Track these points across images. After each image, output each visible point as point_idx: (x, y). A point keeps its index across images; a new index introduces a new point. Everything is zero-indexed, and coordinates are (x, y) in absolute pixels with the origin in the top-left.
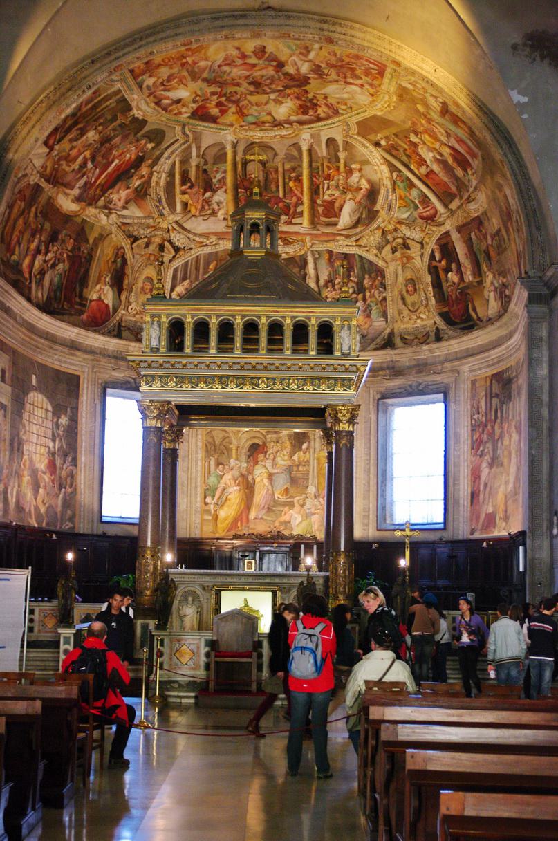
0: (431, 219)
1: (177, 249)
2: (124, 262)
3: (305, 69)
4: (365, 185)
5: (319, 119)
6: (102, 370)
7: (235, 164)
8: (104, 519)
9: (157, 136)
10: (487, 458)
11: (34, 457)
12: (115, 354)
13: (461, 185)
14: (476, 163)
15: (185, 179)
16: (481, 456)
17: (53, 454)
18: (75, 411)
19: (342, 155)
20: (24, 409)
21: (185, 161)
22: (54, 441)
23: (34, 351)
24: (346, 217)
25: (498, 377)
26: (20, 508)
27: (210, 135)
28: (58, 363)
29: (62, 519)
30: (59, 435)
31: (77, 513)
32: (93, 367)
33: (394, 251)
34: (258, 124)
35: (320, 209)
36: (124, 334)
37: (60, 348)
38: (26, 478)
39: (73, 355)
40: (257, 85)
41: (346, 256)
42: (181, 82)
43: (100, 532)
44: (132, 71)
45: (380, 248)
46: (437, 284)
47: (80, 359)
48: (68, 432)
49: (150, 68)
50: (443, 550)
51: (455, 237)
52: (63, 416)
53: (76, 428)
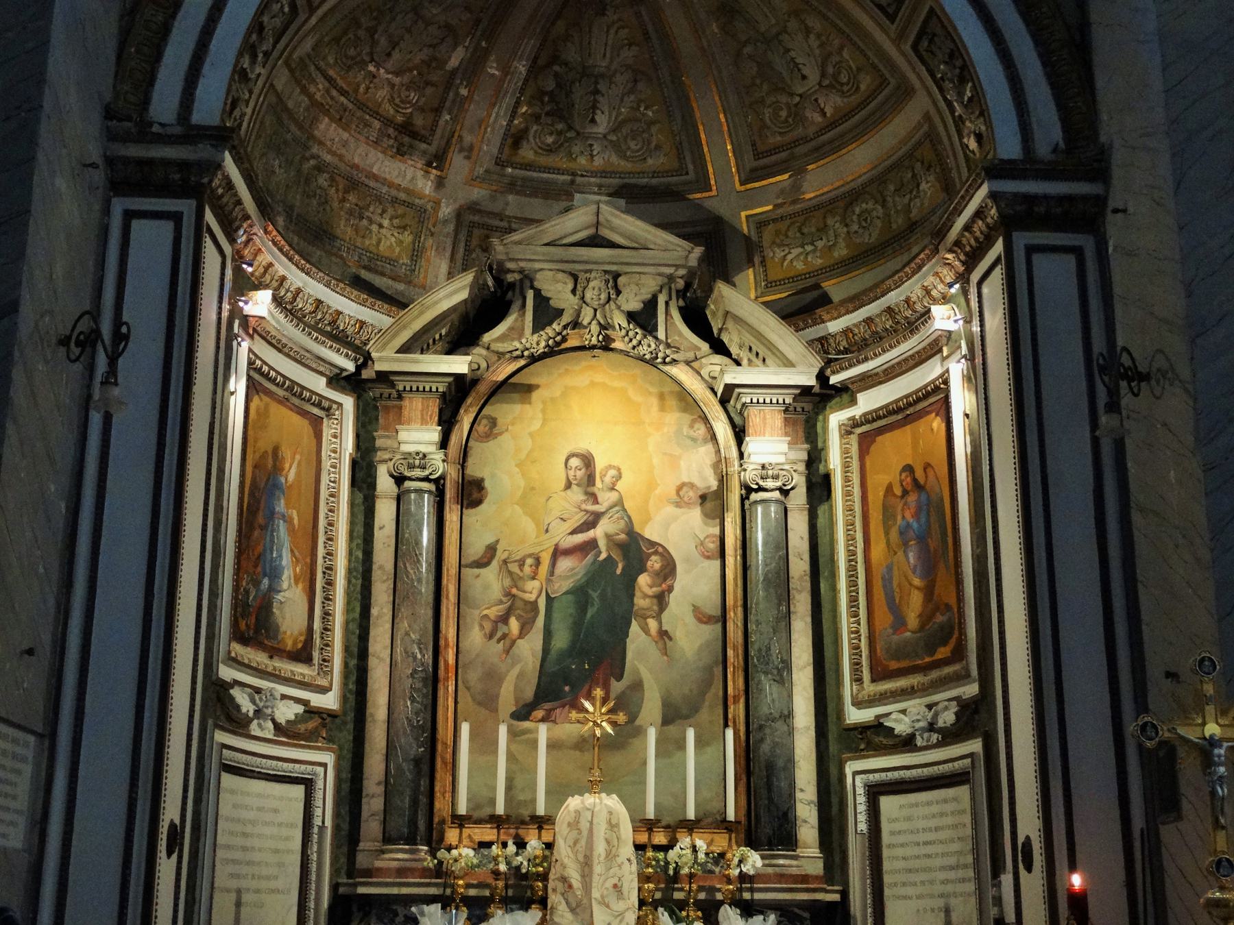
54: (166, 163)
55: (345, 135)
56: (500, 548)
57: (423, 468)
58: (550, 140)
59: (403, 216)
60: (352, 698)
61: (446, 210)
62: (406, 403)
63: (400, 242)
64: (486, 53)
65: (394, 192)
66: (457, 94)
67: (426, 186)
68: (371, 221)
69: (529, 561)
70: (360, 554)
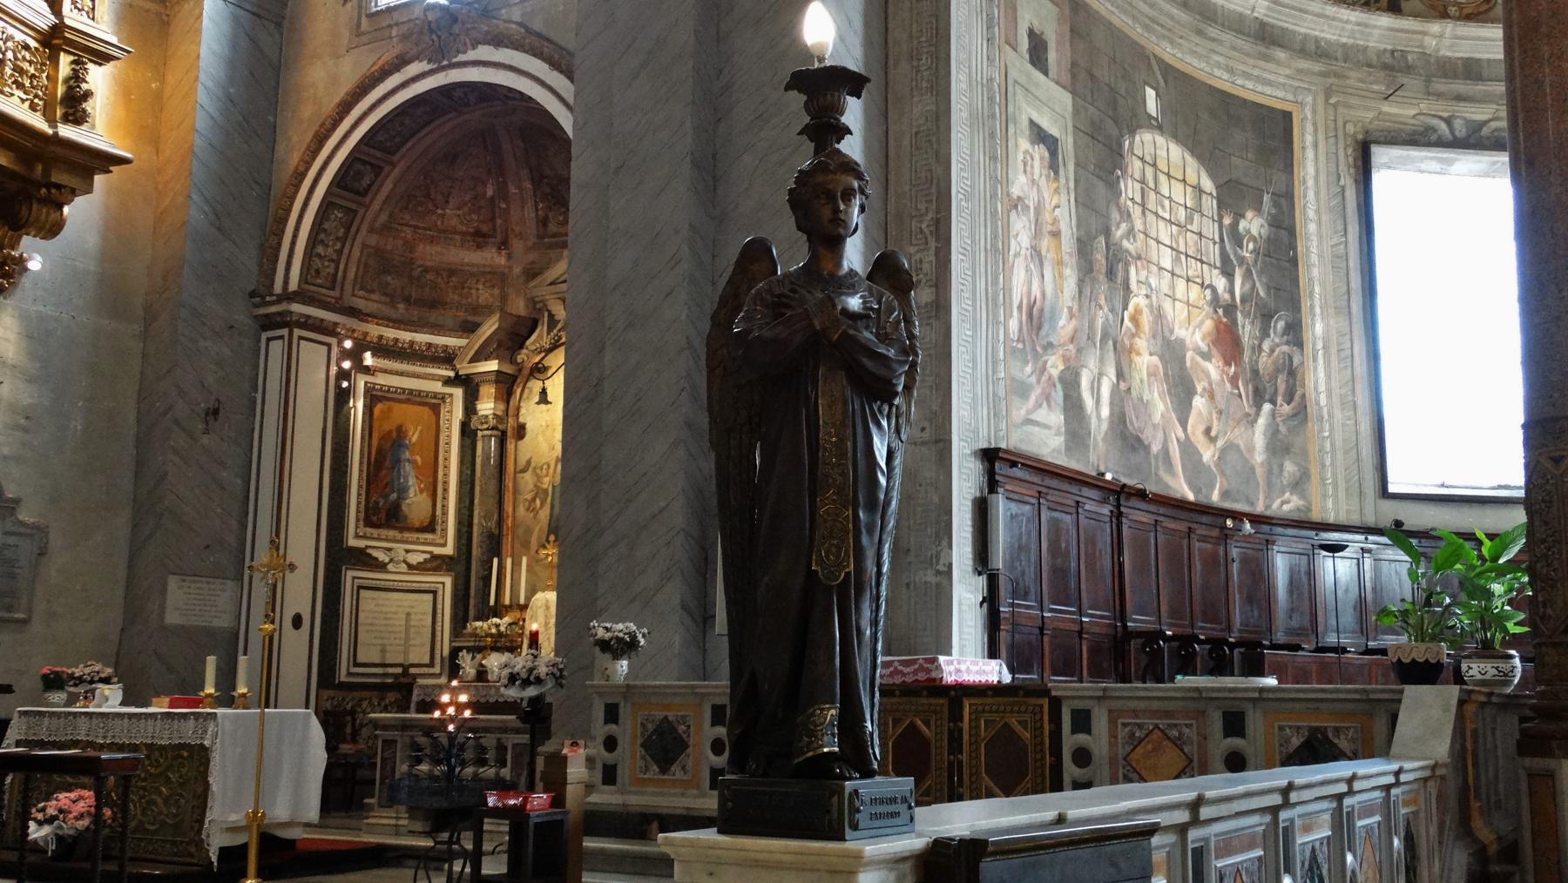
6: (1354, 101)
8: (1392, 489)
11: (1167, 305)
12: (1387, 59)
17: (1230, 309)
18: (1283, 201)
20: (1124, 172)
22: (1228, 274)
23: (1146, 27)
26: (1127, 438)
28: (1225, 76)
29: (1269, 485)
30: (1242, 260)
31: (1314, 471)
32: (1328, 93)
37: (1228, 37)
38: (1145, 360)
39: (1266, 58)
43: (1386, 522)
47: (1288, 72)
48: (1267, 255)
52: (1249, 214)
53: (1295, 249)
54: (273, 314)
55: (439, 249)
56: (533, 460)
57: (486, 423)
58: (561, 218)
59: (490, 281)
60: (464, 548)
61: (517, 270)
62: (481, 388)
63: (492, 295)
64: (505, 183)
65: (482, 269)
66: (500, 208)
67: (502, 261)
68: (470, 288)
69: (545, 467)
70: (469, 472)
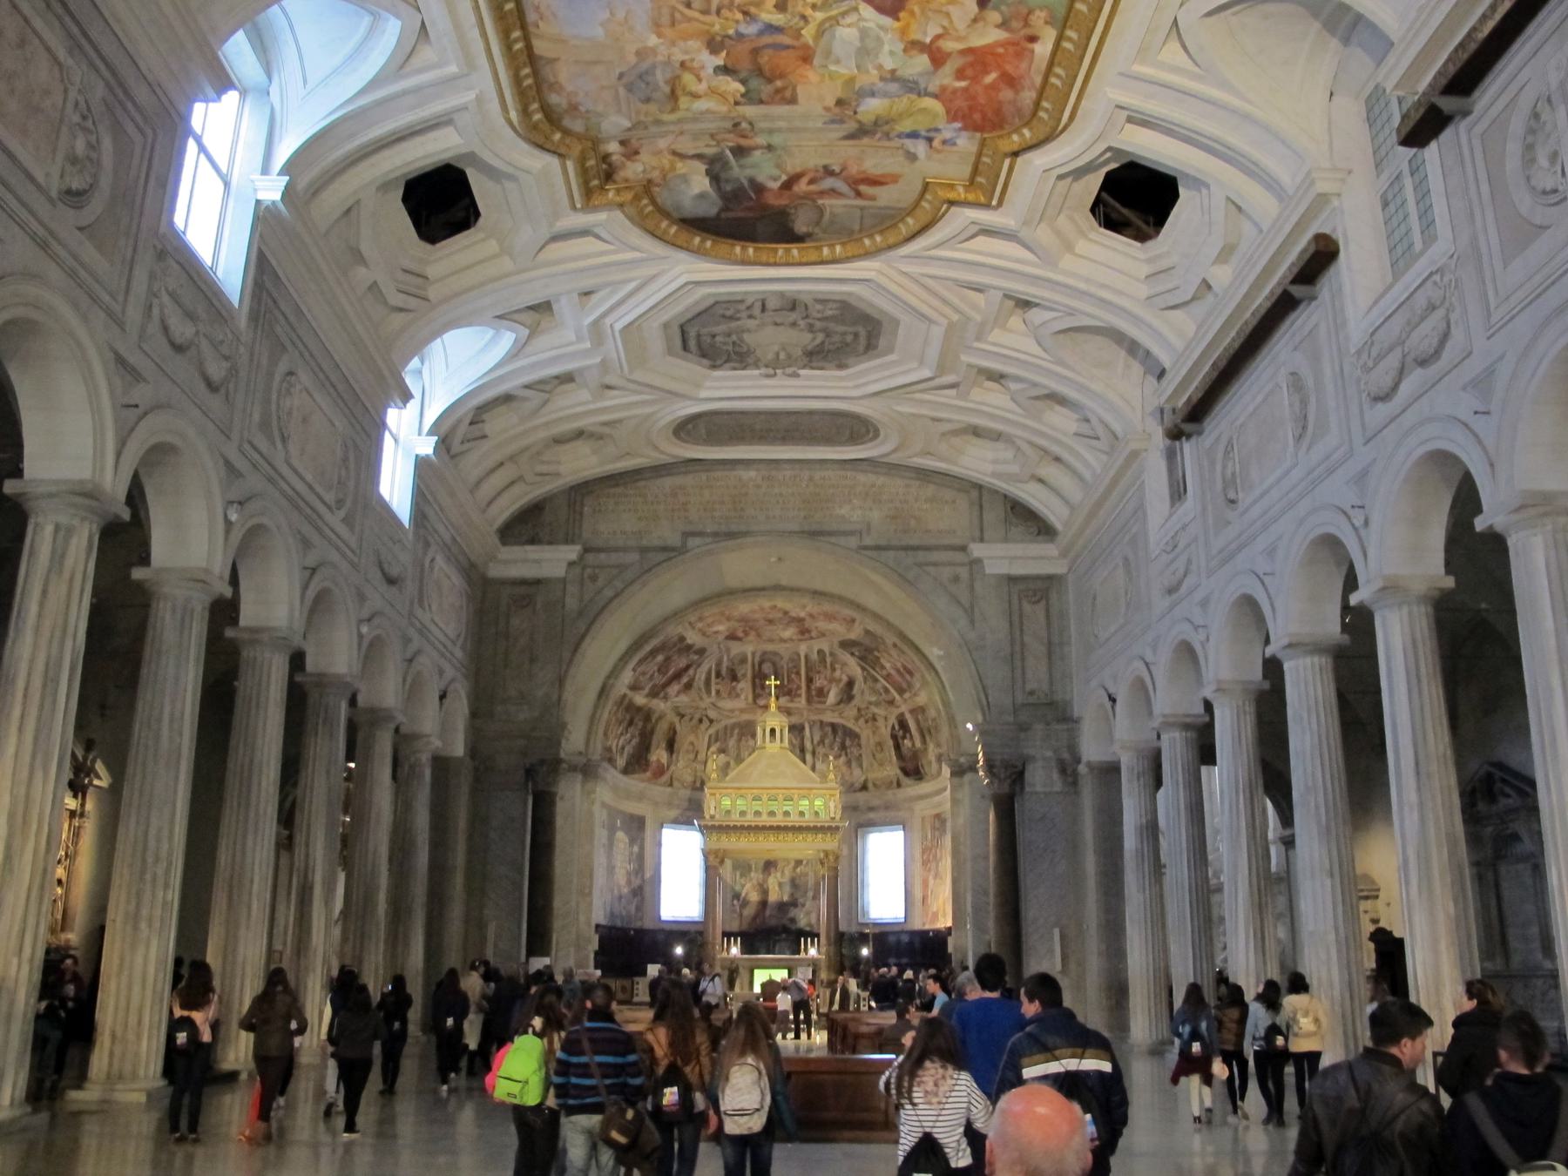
0: (891, 702)
1: (711, 721)
2: (675, 732)
3: (802, 614)
4: (845, 679)
5: (812, 638)
7: (753, 665)
9: (701, 652)
10: (932, 873)
13: (910, 685)
14: (917, 676)
15: (718, 675)
16: (929, 870)
19: (829, 660)
21: (719, 664)
24: (832, 697)
25: (938, 816)
27: (736, 648)
33: (867, 722)
34: (771, 641)
35: (814, 693)
36: (676, 783)
40: (771, 622)
41: (834, 727)
42: (720, 622)
44: (690, 623)
45: (857, 719)
46: (897, 747)
49: (701, 619)
50: (905, 938)
51: (908, 717)
